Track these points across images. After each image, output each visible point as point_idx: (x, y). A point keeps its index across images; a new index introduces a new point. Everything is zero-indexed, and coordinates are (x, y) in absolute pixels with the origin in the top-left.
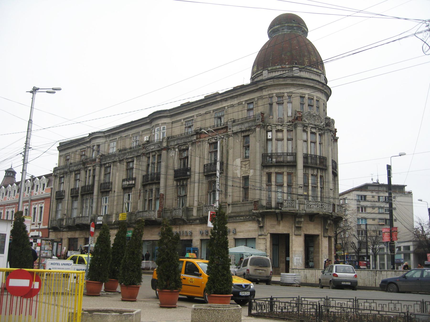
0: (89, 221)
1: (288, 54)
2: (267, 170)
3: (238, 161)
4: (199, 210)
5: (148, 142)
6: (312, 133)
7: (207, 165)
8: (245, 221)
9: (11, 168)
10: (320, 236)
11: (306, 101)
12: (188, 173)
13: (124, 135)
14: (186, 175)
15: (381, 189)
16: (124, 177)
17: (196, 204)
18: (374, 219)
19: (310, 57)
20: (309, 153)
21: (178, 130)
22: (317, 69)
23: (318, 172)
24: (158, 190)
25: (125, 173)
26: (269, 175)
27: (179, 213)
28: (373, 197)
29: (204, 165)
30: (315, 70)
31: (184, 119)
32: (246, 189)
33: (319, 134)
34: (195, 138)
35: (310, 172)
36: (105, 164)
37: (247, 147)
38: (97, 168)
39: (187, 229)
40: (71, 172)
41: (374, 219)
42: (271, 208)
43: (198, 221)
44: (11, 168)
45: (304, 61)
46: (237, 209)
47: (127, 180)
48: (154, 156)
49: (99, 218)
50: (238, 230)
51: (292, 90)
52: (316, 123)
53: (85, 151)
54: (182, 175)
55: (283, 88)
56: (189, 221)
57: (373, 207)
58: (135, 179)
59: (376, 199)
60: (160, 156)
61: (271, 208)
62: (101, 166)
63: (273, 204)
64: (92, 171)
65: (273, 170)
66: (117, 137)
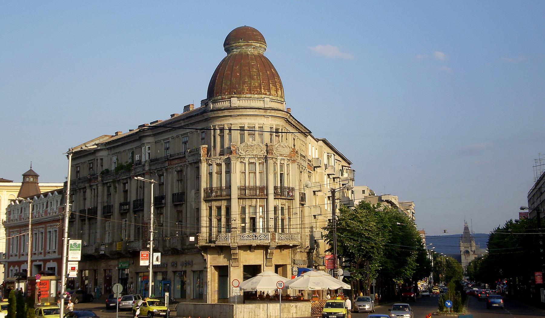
0: (94, 251)
1: (229, 83)
2: (209, 204)
6: (250, 163)
7: (175, 194)
9: (31, 170)
10: (262, 266)
12: (163, 201)
14: (162, 204)
19: (250, 84)
20: (247, 185)
22: (259, 94)
23: (256, 202)
26: (210, 208)
29: (173, 194)
30: (256, 96)
31: (164, 140)
33: (259, 163)
35: (248, 203)
36: (107, 183)
38: (100, 188)
40: (80, 189)
43: (170, 253)
44: (31, 170)
45: (243, 89)
49: (103, 247)
50: (194, 262)
51: (232, 121)
52: (255, 153)
53: (92, 163)
55: (223, 120)
62: (104, 184)
64: (96, 190)
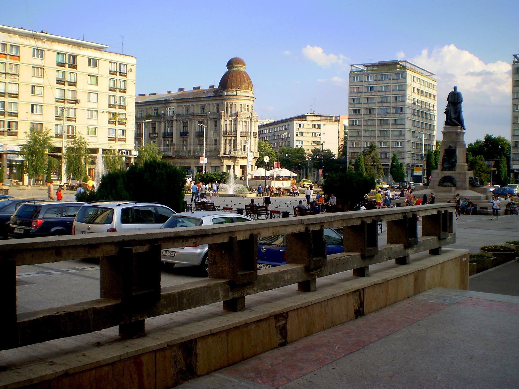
3: (212, 132)
4: (194, 152)
5: (164, 114)
8: (216, 159)
11: (243, 106)
13: (148, 107)
15: (316, 118)
16: (151, 132)
17: (192, 150)
18: (308, 141)
21: (182, 111)
24: (172, 141)
25: (151, 129)
26: (226, 140)
27: (184, 154)
28: (308, 125)
32: (216, 144)
34: (191, 117)
37: (216, 126)
39: (187, 161)
41: (308, 141)
42: (226, 154)
46: (212, 154)
47: (152, 134)
48: (168, 123)
54: (184, 135)
56: (190, 158)
57: (308, 133)
58: (157, 134)
59: (311, 126)
60: (172, 123)
61: (226, 154)
63: (227, 153)
65: (228, 138)
66: (143, 107)
